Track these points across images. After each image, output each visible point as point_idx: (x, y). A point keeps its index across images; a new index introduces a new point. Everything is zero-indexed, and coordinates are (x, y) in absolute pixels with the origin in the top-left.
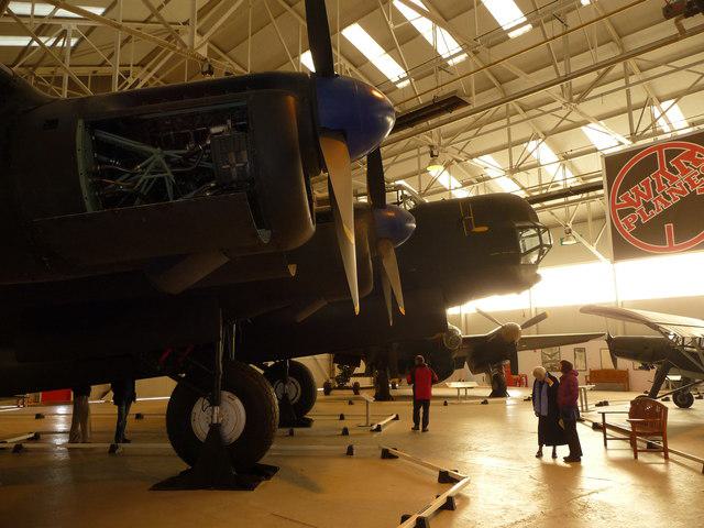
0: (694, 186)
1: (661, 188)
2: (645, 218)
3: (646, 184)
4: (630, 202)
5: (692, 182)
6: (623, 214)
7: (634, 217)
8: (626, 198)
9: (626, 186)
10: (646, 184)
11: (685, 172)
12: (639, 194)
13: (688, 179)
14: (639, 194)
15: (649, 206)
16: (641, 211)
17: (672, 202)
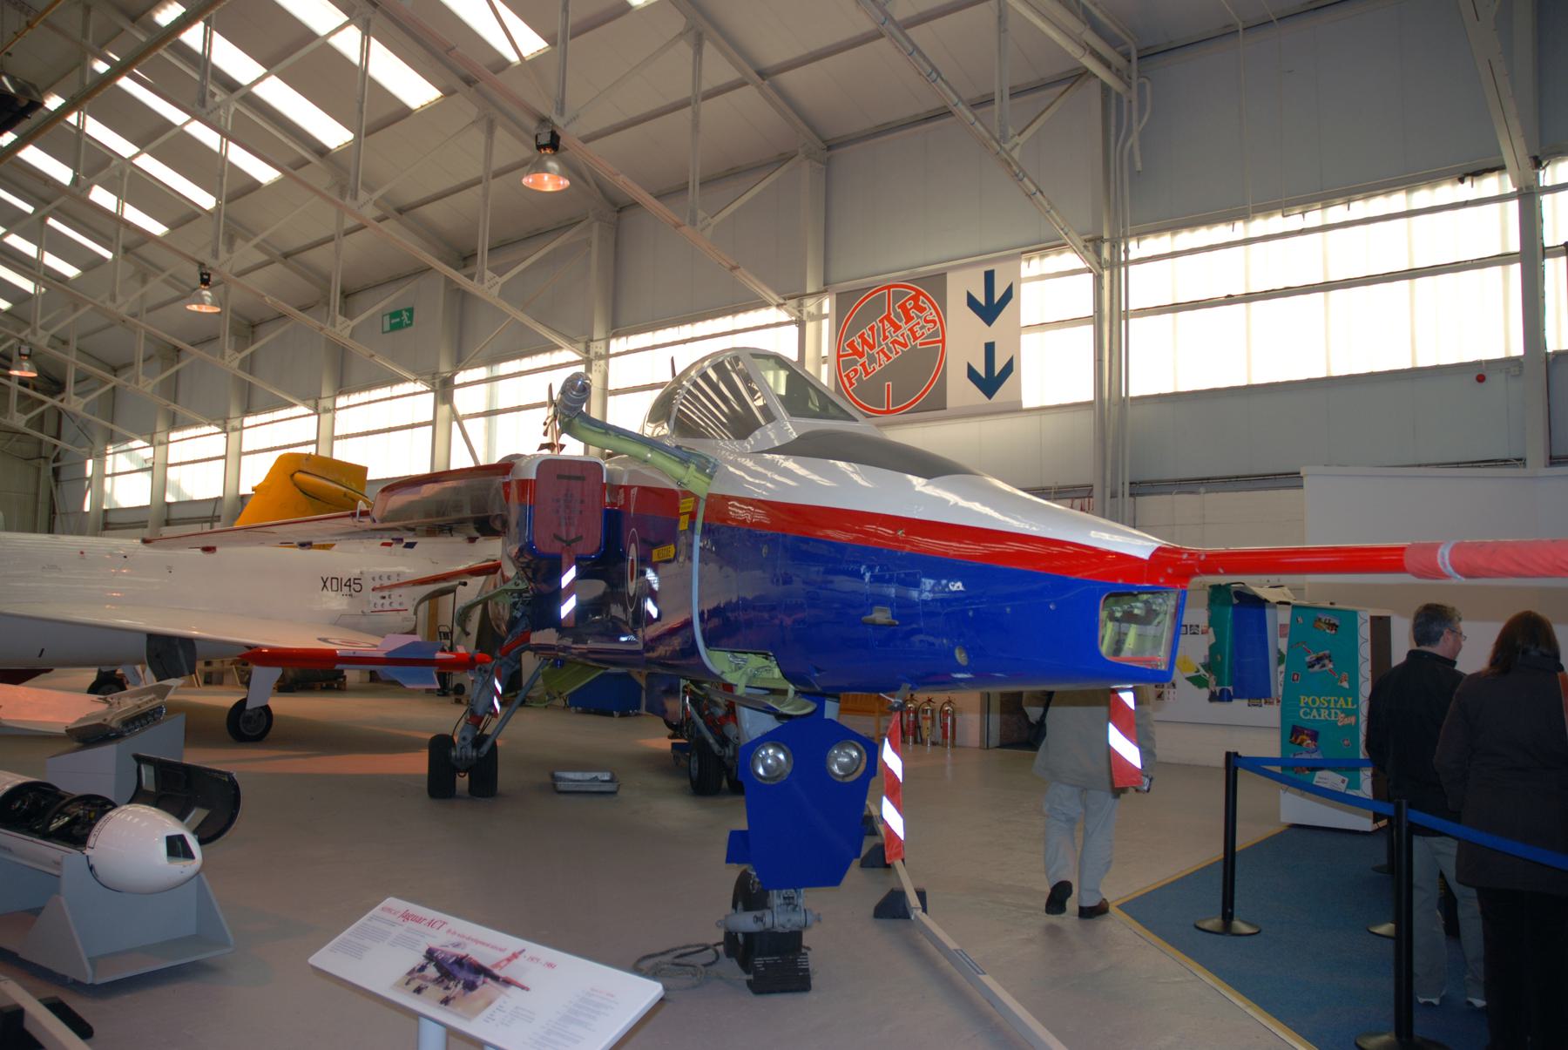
0: (915, 338)
1: (886, 338)
2: (867, 374)
3: (872, 329)
4: (856, 352)
5: (913, 333)
6: (848, 364)
7: (856, 371)
8: (851, 345)
9: (849, 336)
10: (872, 329)
11: (909, 319)
12: (865, 342)
13: (911, 330)
14: (865, 342)
15: (872, 359)
16: (863, 365)
17: (893, 356)
